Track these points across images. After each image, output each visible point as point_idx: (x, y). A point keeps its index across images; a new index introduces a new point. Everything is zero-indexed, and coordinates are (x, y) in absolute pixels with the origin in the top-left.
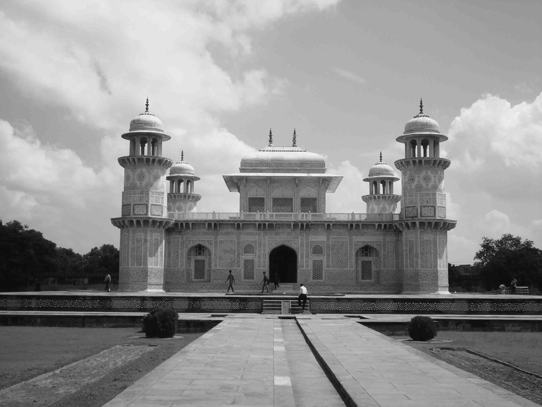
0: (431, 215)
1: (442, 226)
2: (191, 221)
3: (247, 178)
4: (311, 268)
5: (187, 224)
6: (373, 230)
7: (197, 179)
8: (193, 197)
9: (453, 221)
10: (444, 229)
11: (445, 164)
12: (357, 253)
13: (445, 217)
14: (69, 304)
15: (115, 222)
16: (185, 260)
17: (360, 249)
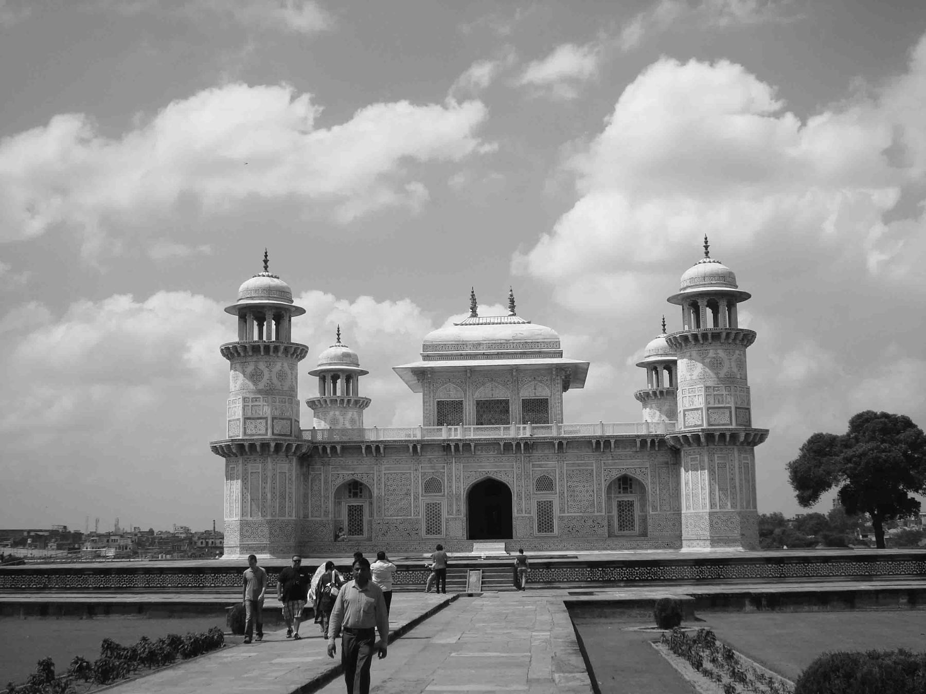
0: (726, 422)
1: (742, 439)
2: (338, 443)
3: (432, 370)
4: (534, 514)
5: (333, 448)
6: (634, 449)
7: (364, 373)
8: (356, 402)
9: (761, 430)
10: (749, 444)
11: (748, 337)
12: (609, 488)
13: (750, 425)
14: (113, 581)
15: (216, 450)
16: (331, 506)
17: (614, 481)
